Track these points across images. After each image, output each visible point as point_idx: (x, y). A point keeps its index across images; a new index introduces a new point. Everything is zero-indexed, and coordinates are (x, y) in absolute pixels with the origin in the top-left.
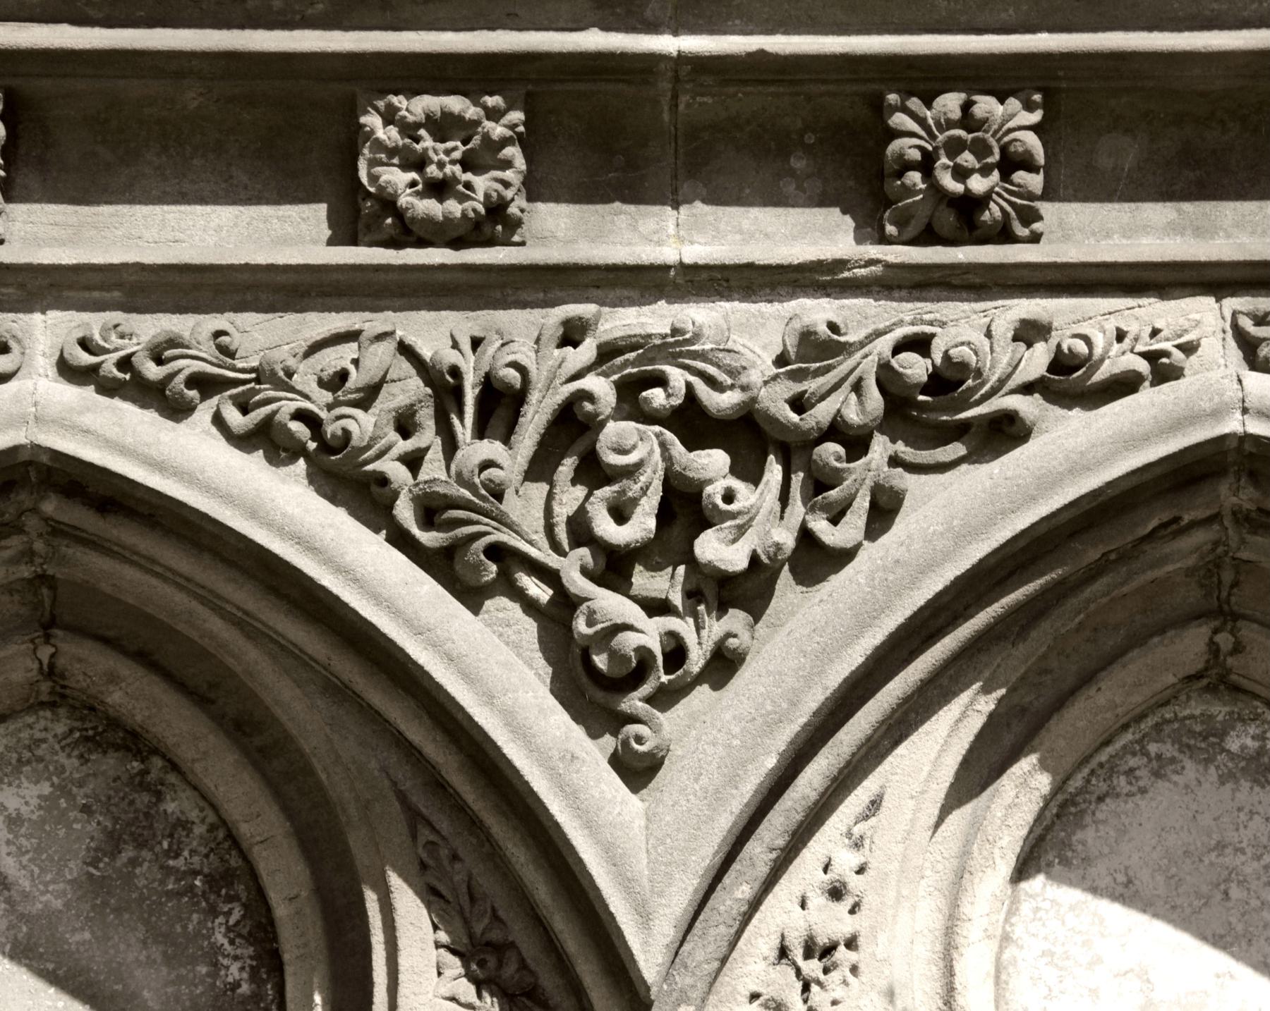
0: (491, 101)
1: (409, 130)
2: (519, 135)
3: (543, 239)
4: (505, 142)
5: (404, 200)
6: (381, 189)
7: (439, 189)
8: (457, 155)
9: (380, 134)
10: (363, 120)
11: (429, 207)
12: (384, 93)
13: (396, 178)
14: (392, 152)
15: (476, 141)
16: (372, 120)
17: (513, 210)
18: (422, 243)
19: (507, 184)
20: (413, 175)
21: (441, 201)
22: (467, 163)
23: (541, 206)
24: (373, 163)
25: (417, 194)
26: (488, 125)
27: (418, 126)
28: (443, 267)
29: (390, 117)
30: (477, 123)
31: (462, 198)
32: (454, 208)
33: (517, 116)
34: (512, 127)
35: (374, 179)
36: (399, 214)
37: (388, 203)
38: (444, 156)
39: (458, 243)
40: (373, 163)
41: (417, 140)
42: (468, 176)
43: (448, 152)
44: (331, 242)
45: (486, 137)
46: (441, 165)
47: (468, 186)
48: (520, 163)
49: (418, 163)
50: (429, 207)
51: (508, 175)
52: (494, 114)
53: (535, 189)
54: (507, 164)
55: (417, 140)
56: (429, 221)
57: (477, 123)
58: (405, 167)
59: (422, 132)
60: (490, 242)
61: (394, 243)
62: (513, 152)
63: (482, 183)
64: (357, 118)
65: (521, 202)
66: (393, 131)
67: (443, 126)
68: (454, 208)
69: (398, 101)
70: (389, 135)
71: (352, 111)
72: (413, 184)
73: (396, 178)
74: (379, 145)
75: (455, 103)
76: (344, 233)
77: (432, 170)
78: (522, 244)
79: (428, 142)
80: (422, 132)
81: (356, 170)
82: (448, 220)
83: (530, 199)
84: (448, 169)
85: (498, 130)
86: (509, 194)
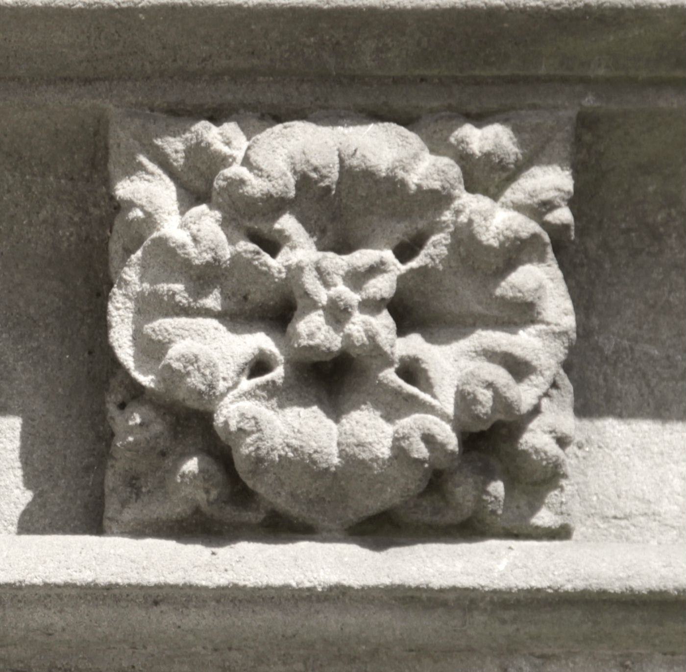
0: (485, 138)
1: (253, 219)
2: (557, 232)
3: (618, 521)
4: (516, 252)
5: (231, 412)
6: (172, 377)
7: (330, 379)
8: (383, 286)
9: (173, 226)
10: (124, 189)
11: (304, 430)
12: (182, 114)
13: (213, 349)
14: (204, 276)
15: (435, 249)
16: (148, 191)
17: (536, 438)
18: (280, 527)
19: (519, 368)
20: (260, 341)
21: (335, 412)
22: (407, 311)
23: (612, 428)
24: (150, 307)
25: (271, 391)
26: (471, 204)
27: (276, 205)
28: (338, 596)
29: (198, 183)
30: (439, 199)
31: (395, 406)
32: (370, 431)
33: (552, 180)
34: (538, 210)
35: (151, 349)
36: (219, 449)
37: (190, 421)
38: (342, 289)
39: (379, 529)
40: (150, 307)
41: (272, 245)
42: (413, 345)
43: (357, 278)
44: (29, 524)
45: (465, 239)
46: (337, 314)
47: (411, 371)
48: (559, 309)
49: (277, 311)
50: (304, 430)
51: (525, 342)
52: (487, 176)
53: (597, 382)
54: (522, 313)
55: (272, 245)
56: (301, 465)
57: (439, 199)
58: (237, 318)
59: (288, 223)
60: (471, 528)
61: (199, 528)
62: (540, 280)
63: (453, 365)
64: (108, 183)
65: (559, 416)
66: (207, 221)
67: (342, 208)
68: (370, 431)
69: (223, 137)
70: (198, 233)
71: (93, 166)
72: (259, 366)
73: (213, 349)
74: (168, 259)
75: (381, 146)
76: (72, 498)
77: (313, 329)
78: (561, 533)
79: (301, 250)
80: (288, 223)
81: (102, 325)
82: (354, 465)
83: (585, 409)
84: (358, 325)
85: (496, 219)
86: (525, 394)
